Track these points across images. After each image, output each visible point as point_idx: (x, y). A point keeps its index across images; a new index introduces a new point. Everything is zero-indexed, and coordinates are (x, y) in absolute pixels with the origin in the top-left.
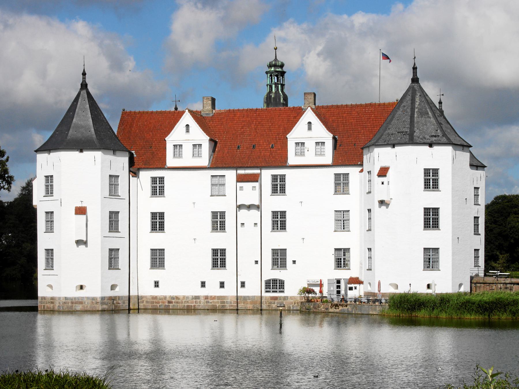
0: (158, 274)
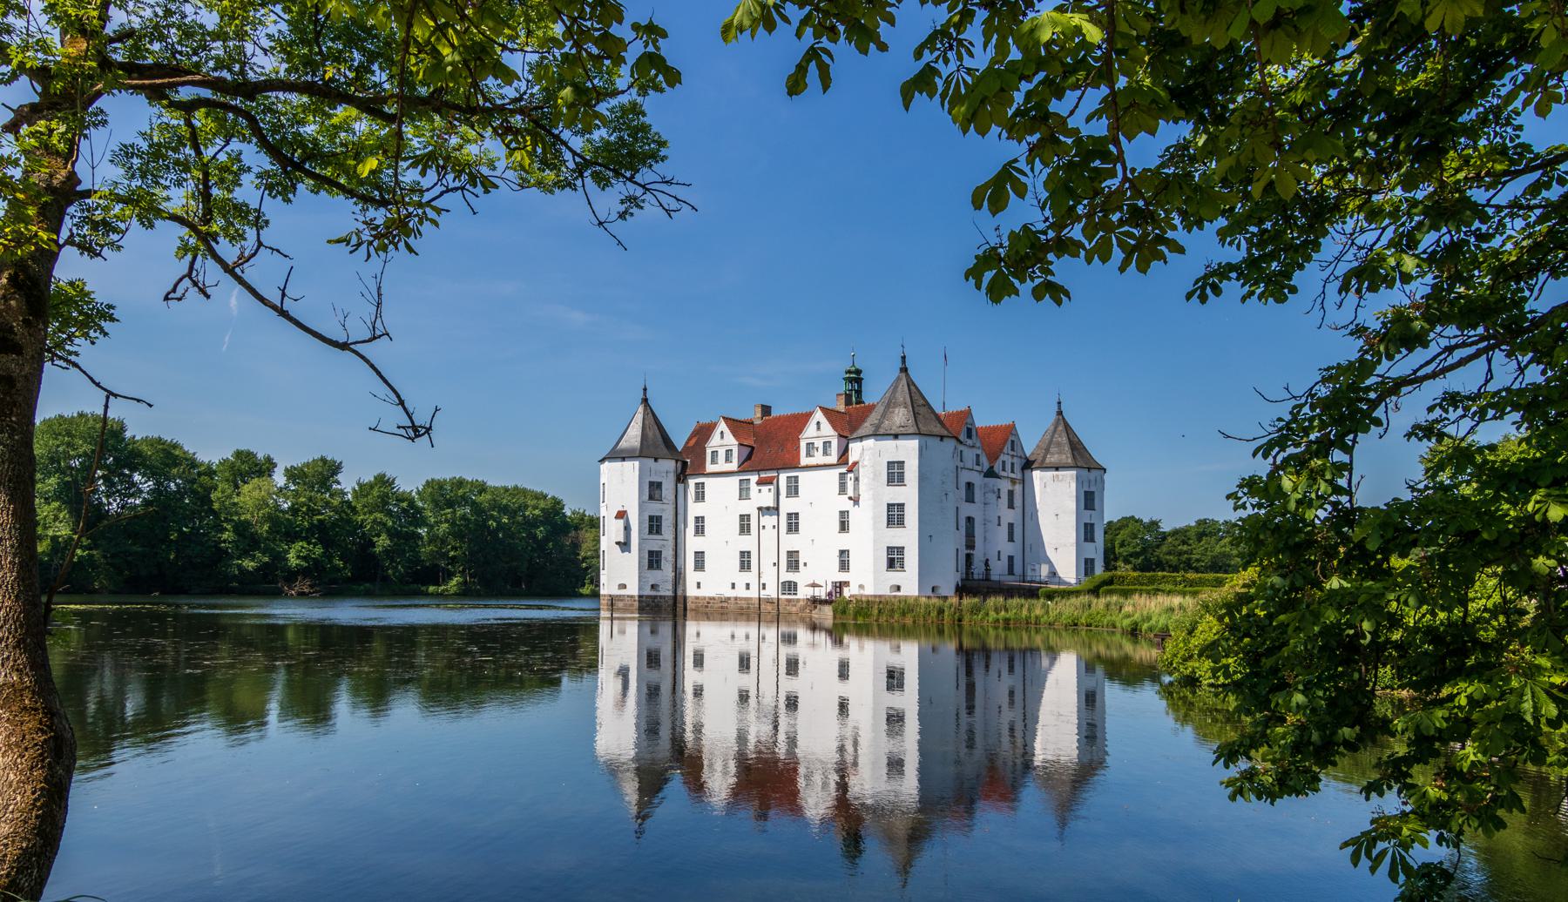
0: (699, 576)
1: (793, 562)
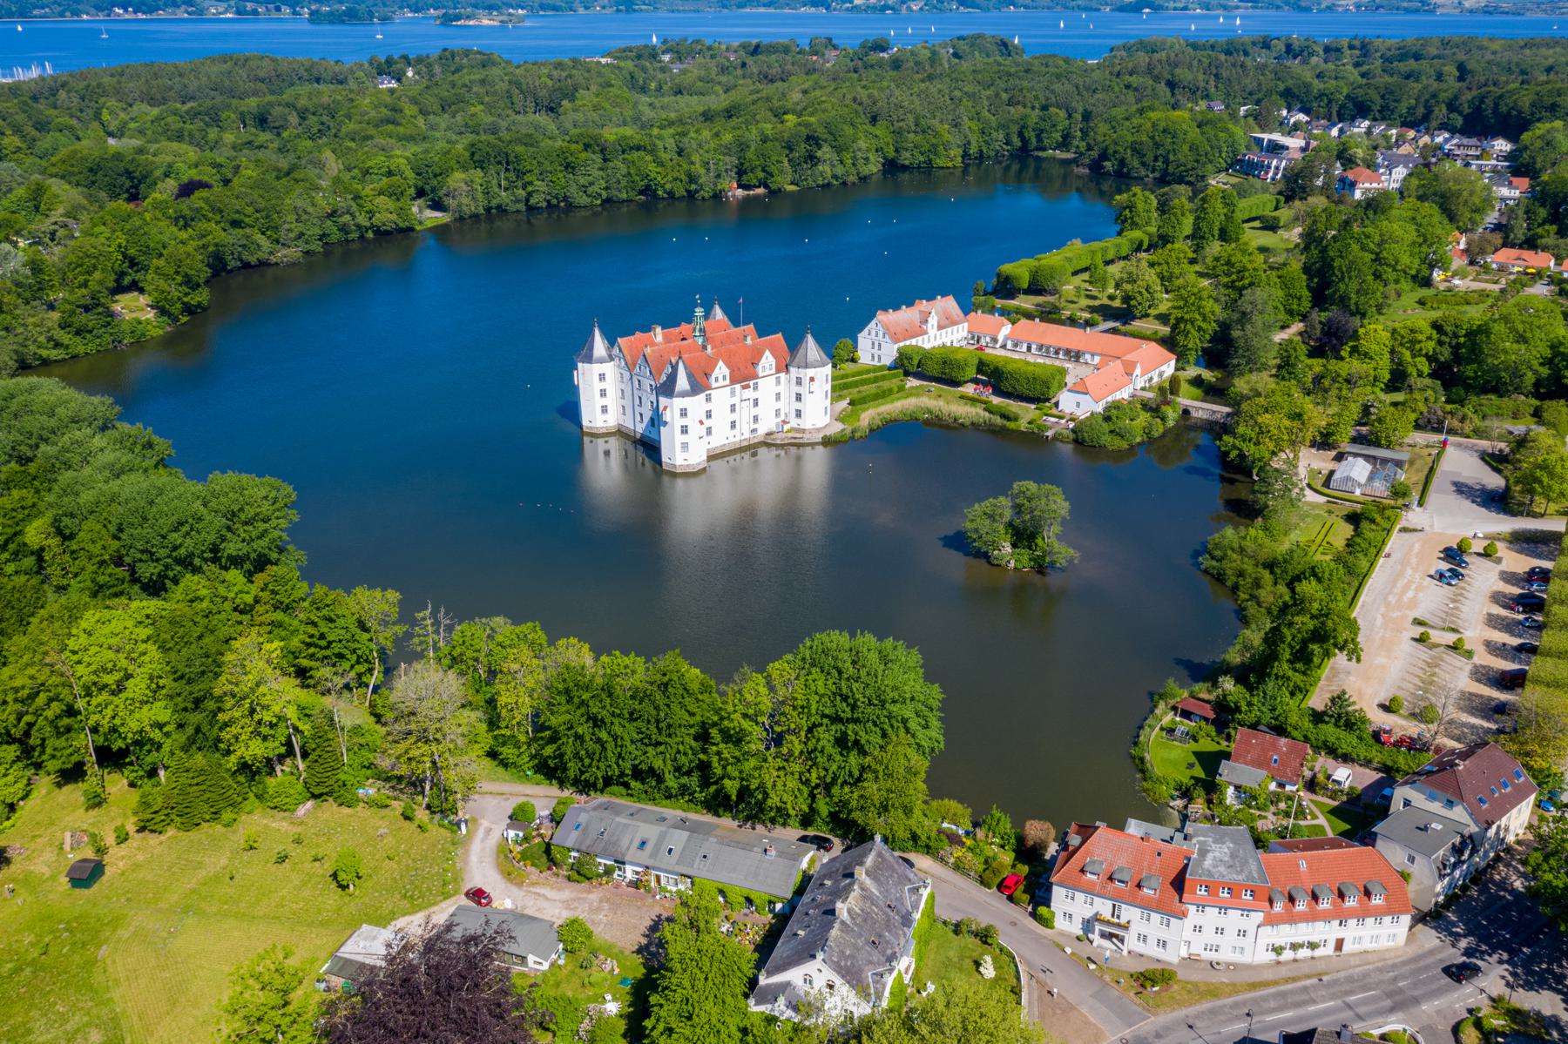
1: (756, 419)
